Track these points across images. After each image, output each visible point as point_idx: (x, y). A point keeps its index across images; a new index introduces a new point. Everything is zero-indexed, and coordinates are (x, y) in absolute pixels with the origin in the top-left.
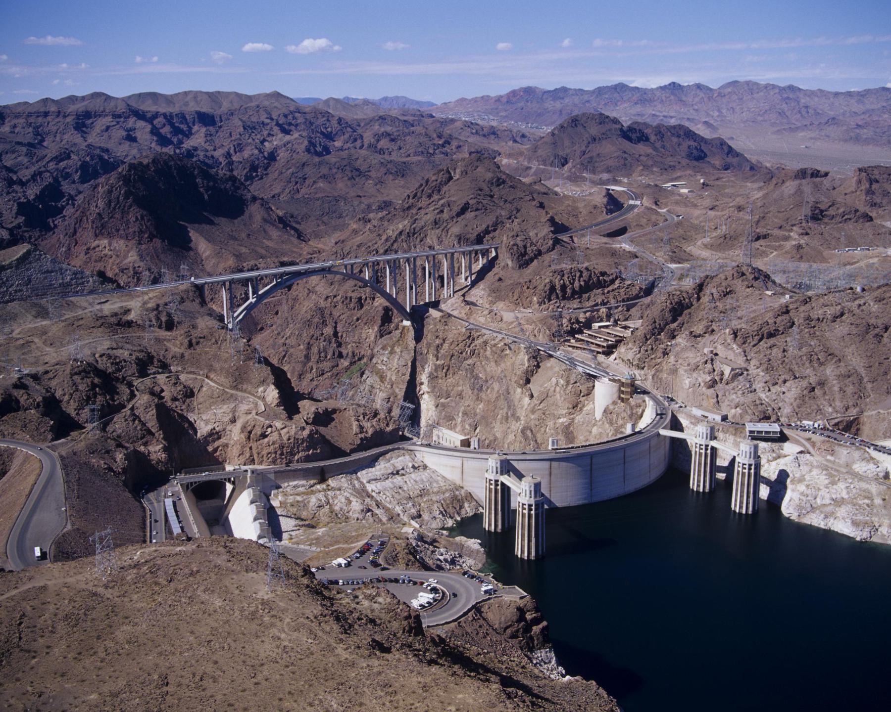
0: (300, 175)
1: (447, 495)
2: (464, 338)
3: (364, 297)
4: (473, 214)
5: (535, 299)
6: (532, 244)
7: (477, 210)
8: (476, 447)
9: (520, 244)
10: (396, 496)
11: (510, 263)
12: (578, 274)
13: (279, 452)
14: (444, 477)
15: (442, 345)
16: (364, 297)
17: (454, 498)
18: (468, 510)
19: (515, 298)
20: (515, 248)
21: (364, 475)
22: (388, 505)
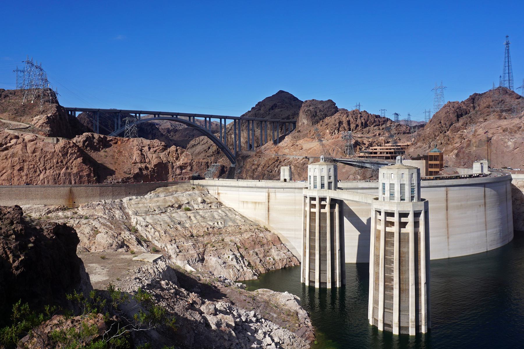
0: (191, 134)
1: (246, 236)
2: (273, 161)
3: (210, 162)
4: (279, 110)
5: (328, 131)
6: (320, 111)
7: (282, 107)
8: (288, 178)
9: (313, 110)
10: (172, 232)
11: (306, 122)
12: (359, 115)
13: (17, 167)
14: (243, 217)
15: (256, 169)
16: (210, 162)
17: (257, 242)
18: (277, 257)
19: (312, 134)
20: (309, 112)
21: (131, 203)
22: (156, 243)
